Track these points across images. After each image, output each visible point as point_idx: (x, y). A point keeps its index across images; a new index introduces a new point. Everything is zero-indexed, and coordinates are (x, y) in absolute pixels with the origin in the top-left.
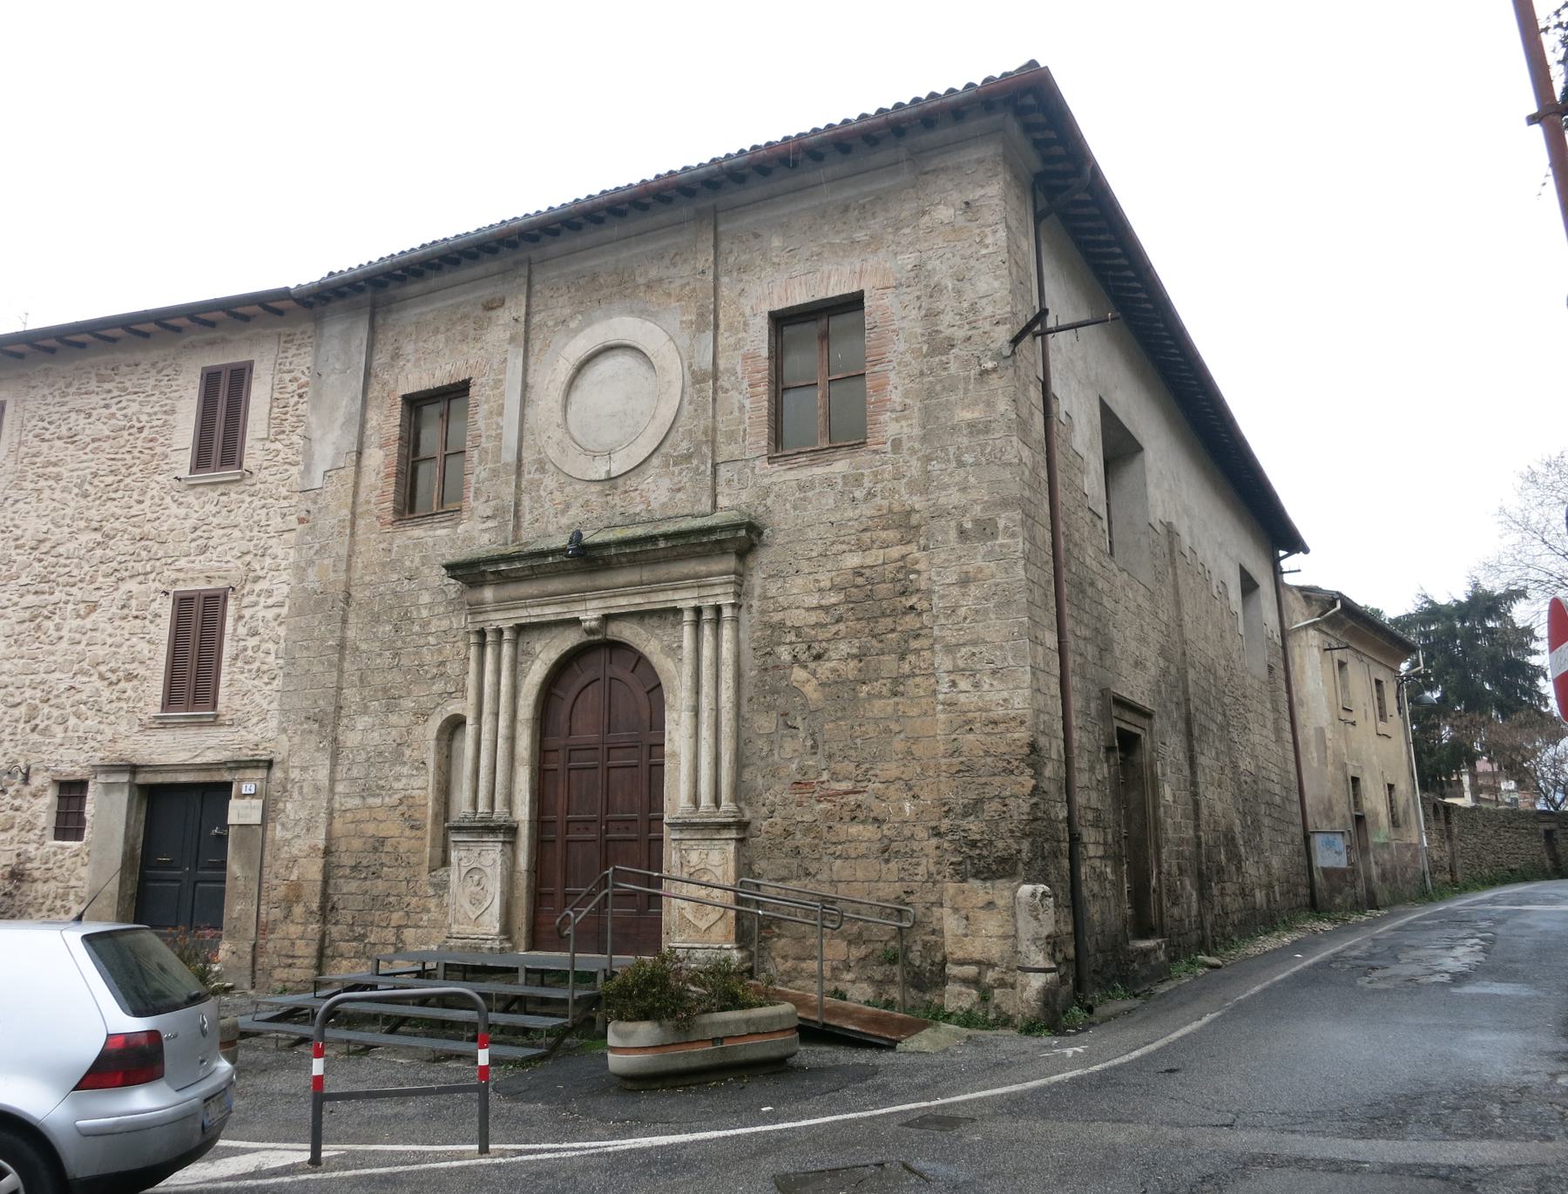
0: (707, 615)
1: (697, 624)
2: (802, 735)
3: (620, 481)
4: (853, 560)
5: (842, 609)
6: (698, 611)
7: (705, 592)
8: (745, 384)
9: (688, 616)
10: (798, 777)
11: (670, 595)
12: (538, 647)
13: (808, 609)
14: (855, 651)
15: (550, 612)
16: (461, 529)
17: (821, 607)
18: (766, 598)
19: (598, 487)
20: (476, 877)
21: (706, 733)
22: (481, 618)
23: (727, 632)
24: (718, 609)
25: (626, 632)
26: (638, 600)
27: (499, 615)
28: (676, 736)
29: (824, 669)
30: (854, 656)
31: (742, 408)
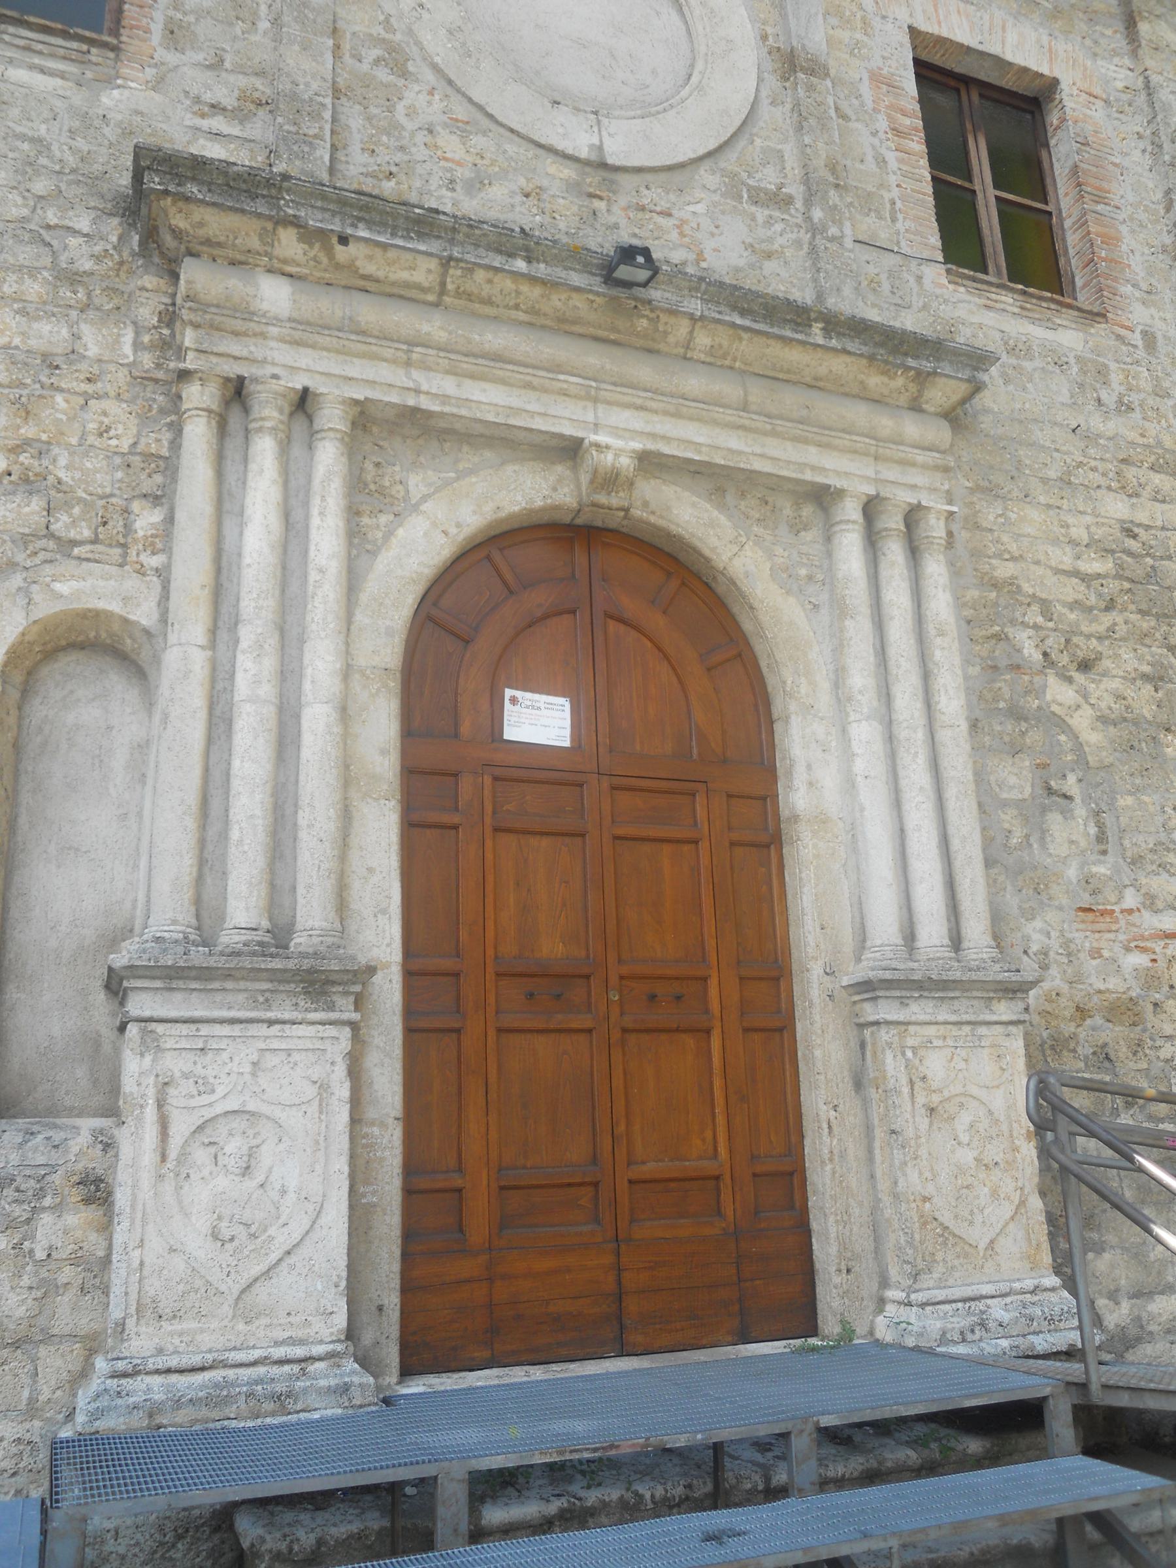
0: (893, 521)
1: (872, 539)
2: (1080, 811)
3: (624, 179)
4: (1117, 508)
5: (1113, 586)
6: (871, 509)
7: (891, 473)
8: (882, 124)
9: (851, 510)
10: (1086, 900)
11: (812, 455)
12: (416, 483)
13: (1058, 571)
14: (1146, 669)
15: (488, 399)
16: (111, 99)
17: (1075, 573)
18: (978, 527)
19: (568, 172)
20: (234, 1147)
21: (916, 774)
22: (235, 348)
23: (935, 568)
24: (913, 516)
25: (686, 514)
26: (734, 441)
27: (305, 358)
28: (829, 778)
29: (1104, 690)
30: (1145, 677)
31: (882, 162)
